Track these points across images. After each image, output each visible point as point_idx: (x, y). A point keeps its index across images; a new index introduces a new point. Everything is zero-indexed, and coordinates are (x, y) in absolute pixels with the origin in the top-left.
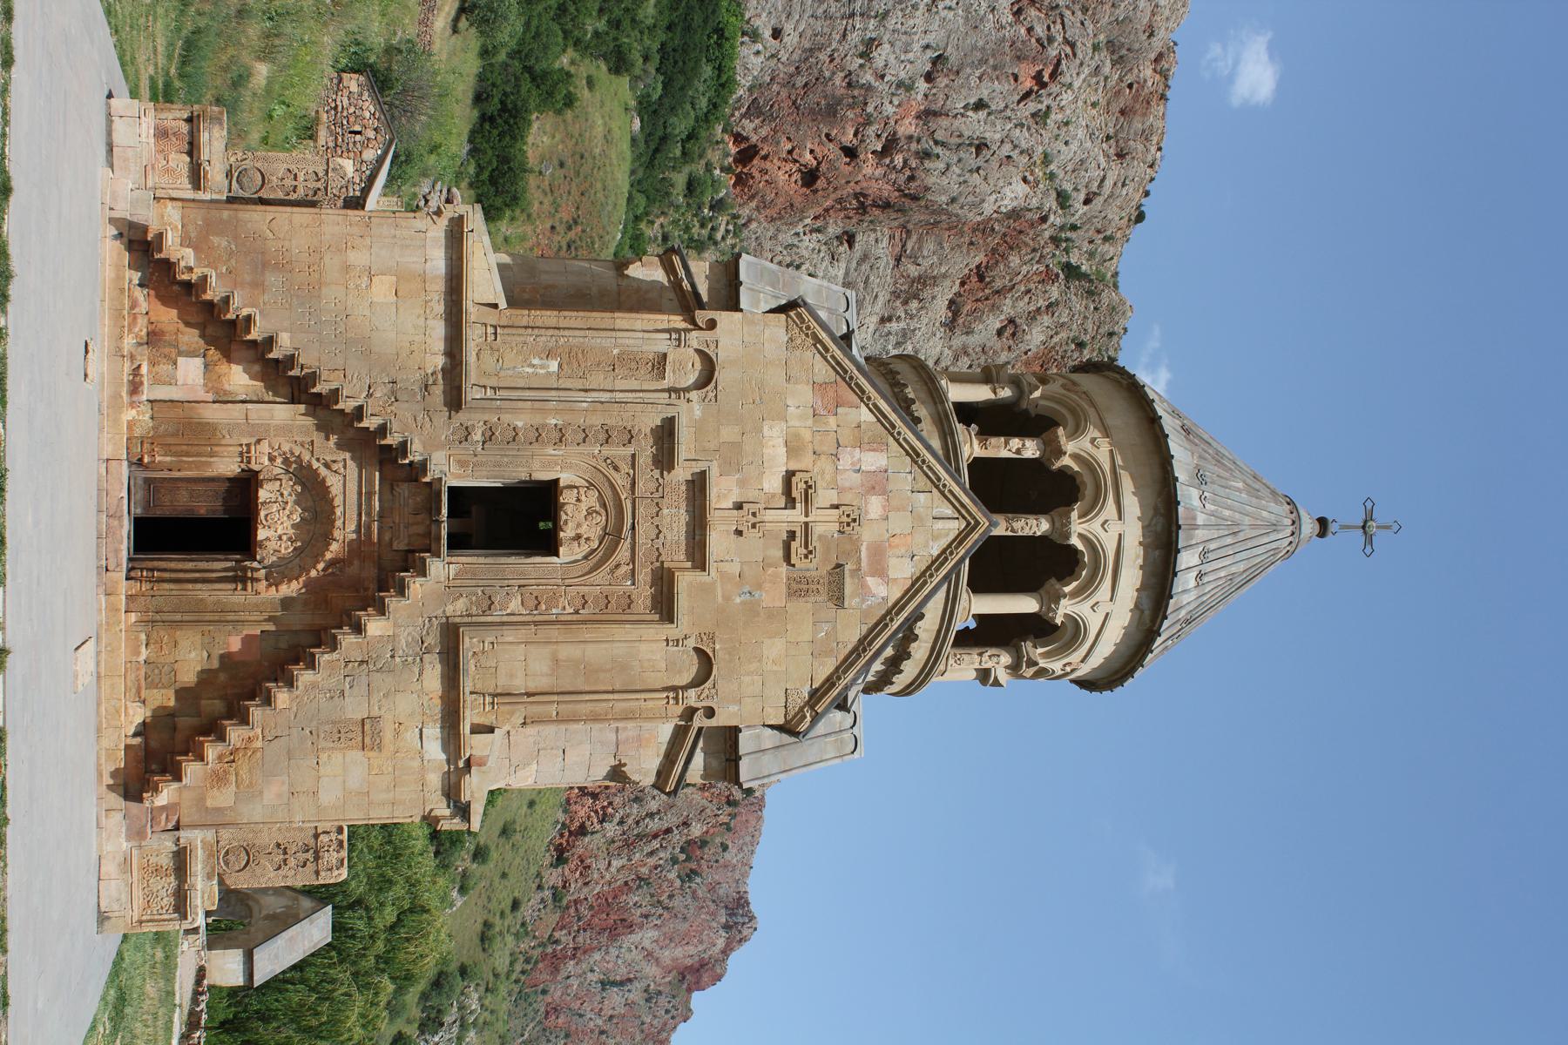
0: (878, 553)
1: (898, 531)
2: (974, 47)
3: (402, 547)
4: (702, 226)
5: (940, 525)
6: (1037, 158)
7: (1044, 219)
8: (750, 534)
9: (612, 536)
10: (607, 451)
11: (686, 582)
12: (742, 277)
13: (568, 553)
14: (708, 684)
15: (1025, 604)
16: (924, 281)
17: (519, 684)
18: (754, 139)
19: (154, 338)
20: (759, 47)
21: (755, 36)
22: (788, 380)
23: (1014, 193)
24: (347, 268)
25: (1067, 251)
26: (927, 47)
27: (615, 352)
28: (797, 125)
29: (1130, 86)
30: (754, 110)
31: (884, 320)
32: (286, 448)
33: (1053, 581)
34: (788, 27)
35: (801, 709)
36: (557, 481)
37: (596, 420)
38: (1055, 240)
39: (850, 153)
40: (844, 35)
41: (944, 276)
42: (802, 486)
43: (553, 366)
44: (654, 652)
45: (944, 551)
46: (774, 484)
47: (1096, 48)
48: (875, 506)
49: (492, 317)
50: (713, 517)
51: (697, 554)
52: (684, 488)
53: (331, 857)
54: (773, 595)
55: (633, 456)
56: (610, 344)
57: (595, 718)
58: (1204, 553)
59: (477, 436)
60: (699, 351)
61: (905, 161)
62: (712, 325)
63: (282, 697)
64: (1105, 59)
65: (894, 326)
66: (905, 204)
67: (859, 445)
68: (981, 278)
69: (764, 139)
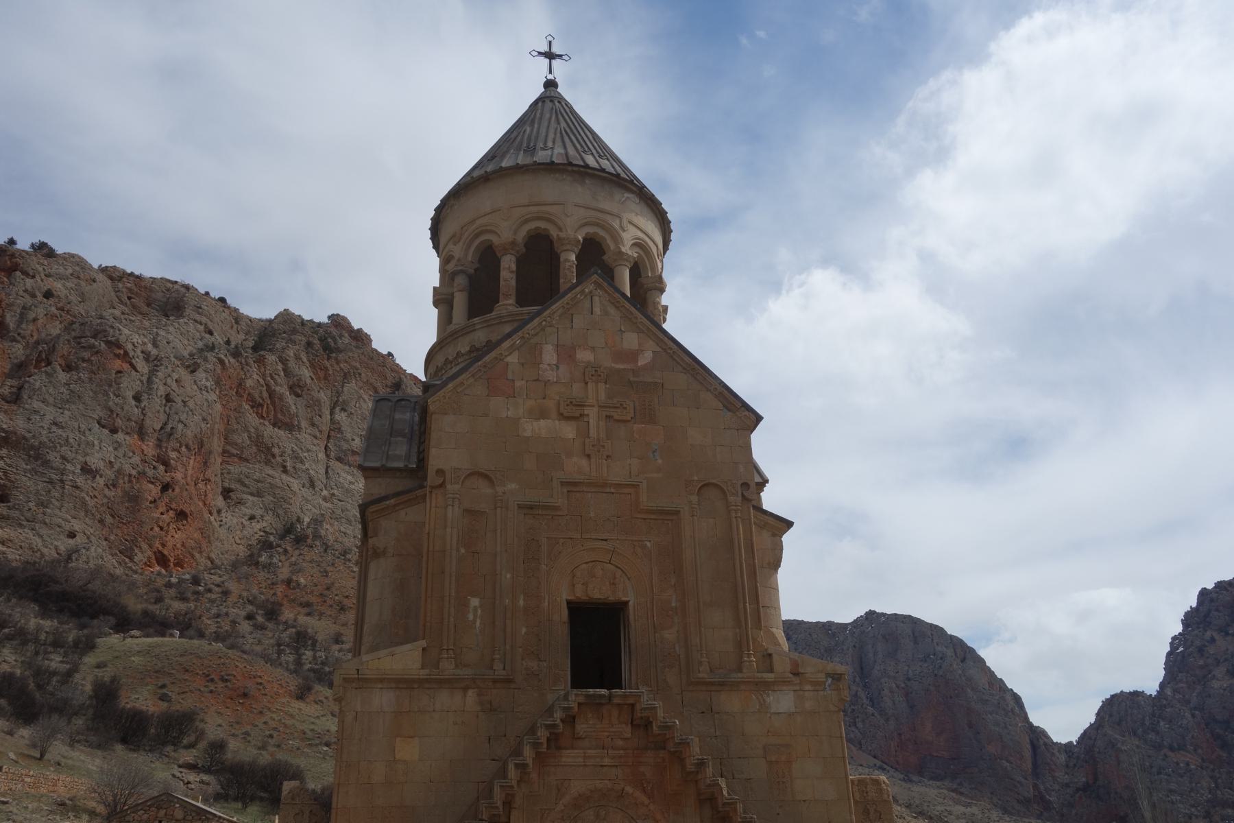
0: (621, 356)
3: (629, 729)
4: (210, 591)
5: (597, 310)
27: (463, 551)
29: (129, 298)
30: (128, 553)
31: (285, 471)
33: (605, 257)
34: (67, 527)
36: (569, 603)
39: (166, 487)
40: (77, 487)
43: (475, 602)
45: (617, 308)
46: (568, 431)
48: (584, 356)
58: (585, 152)
61: (174, 450)
62: (440, 472)
69: (151, 546)
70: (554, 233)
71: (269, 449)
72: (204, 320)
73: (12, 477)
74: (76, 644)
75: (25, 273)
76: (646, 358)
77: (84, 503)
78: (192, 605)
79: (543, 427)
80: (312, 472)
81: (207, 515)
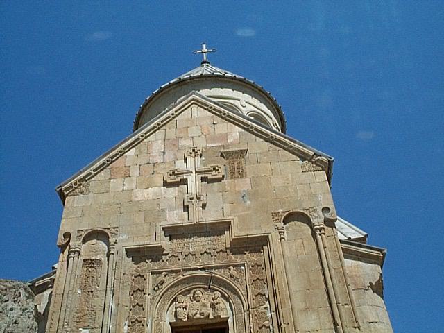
0: (213, 139)
1: (200, 132)
8: (204, 200)
9: (211, 283)
10: (149, 290)
13: (225, 312)
14: (307, 213)
22: (107, 192)
35: (313, 163)
37: (126, 299)
42: (173, 177)
44: (290, 248)
48: (185, 143)
50: (194, 221)
51: (219, 228)
52: (175, 241)
54: (244, 185)
55: (153, 273)
60: (84, 241)
79: (150, 193)
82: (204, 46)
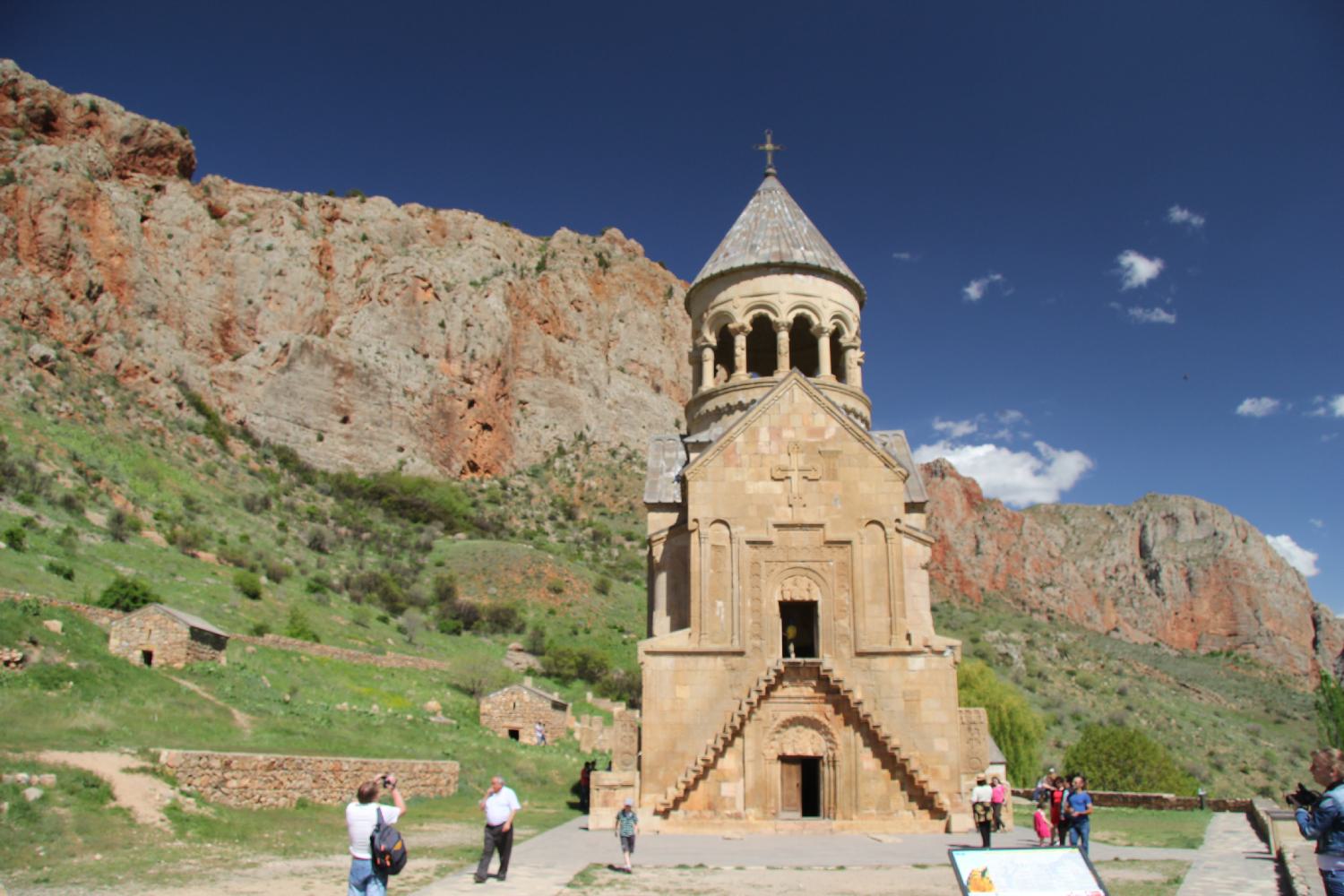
2: (408, 329)
4: (516, 494)
5: (797, 399)
6: (471, 289)
7: (510, 284)
11: (831, 536)
12: (656, 501)
13: (816, 595)
15: (824, 345)
16: (547, 357)
17: (885, 620)
18: (464, 463)
19: (710, 807)
20: (409, 460)
21: (403, 463)
23: (495, 302)
24: (673, 710)
25: (529, 270)
26: (408, 357)
28: (455, 436)
30: (446, 462)
31: (572, 382)
32: (766, 741)
34: (398, 442)
37: (748, 581)
38: (522, 277)
39: (471, 404)
40: (402, 408)
41: (545, 345)
43: (720, 604)
44: (867, 549)
46: (778, 488)
47: (407, 254)
48: (788, 434)
49: (696, 635)
53: (974, 717)
56: (708, 572)
57: (902, 581)
58: (794, 246)
59: (757, 642)
62: (696, 520)
63: (894, 742)
64: (412, 247)
65: (576, 376)
66: (502, 368)
67: (757, 441)
68: (546, 322)
69: (464, 456)
70: (772, 317)
71: (557, 363)
72: (492, 246)
73: (352, 402)
74: (418, 546)
75: (344, 220)
76: (830, 433)
77: (409, 422)
78: (502, 508)
80: (596, 383)
81: (508, 427)
82: (769, 138)
